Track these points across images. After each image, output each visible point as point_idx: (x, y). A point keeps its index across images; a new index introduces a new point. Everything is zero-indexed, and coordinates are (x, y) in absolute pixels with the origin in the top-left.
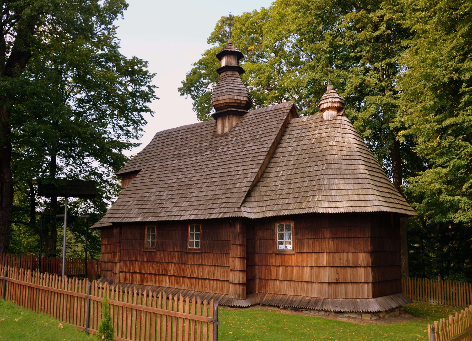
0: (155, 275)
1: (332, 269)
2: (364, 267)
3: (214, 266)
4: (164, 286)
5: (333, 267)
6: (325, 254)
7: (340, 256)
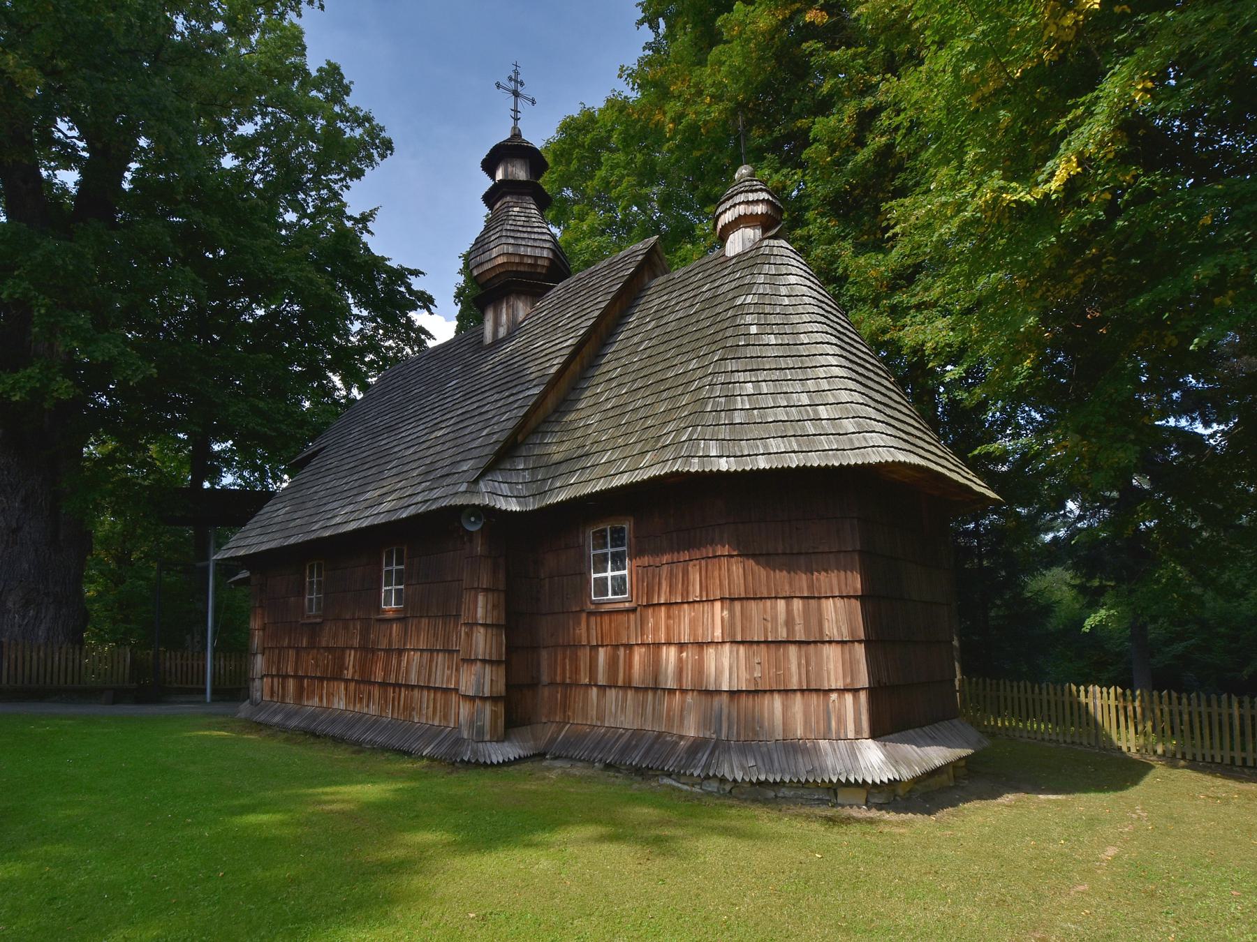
0: (321, 679)
1: (742, 649)
2: (843, 642)
3: (431, 651)
4: (336, 706)
5: (743, 642)
6: (718, 605)
7: (765, 611)
